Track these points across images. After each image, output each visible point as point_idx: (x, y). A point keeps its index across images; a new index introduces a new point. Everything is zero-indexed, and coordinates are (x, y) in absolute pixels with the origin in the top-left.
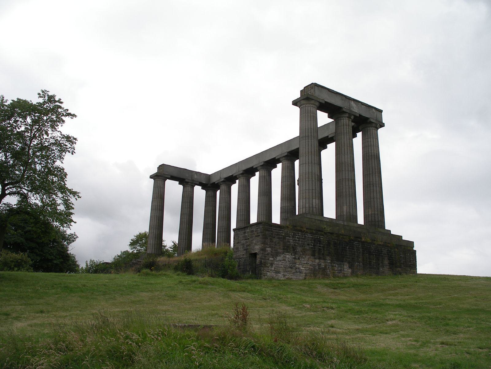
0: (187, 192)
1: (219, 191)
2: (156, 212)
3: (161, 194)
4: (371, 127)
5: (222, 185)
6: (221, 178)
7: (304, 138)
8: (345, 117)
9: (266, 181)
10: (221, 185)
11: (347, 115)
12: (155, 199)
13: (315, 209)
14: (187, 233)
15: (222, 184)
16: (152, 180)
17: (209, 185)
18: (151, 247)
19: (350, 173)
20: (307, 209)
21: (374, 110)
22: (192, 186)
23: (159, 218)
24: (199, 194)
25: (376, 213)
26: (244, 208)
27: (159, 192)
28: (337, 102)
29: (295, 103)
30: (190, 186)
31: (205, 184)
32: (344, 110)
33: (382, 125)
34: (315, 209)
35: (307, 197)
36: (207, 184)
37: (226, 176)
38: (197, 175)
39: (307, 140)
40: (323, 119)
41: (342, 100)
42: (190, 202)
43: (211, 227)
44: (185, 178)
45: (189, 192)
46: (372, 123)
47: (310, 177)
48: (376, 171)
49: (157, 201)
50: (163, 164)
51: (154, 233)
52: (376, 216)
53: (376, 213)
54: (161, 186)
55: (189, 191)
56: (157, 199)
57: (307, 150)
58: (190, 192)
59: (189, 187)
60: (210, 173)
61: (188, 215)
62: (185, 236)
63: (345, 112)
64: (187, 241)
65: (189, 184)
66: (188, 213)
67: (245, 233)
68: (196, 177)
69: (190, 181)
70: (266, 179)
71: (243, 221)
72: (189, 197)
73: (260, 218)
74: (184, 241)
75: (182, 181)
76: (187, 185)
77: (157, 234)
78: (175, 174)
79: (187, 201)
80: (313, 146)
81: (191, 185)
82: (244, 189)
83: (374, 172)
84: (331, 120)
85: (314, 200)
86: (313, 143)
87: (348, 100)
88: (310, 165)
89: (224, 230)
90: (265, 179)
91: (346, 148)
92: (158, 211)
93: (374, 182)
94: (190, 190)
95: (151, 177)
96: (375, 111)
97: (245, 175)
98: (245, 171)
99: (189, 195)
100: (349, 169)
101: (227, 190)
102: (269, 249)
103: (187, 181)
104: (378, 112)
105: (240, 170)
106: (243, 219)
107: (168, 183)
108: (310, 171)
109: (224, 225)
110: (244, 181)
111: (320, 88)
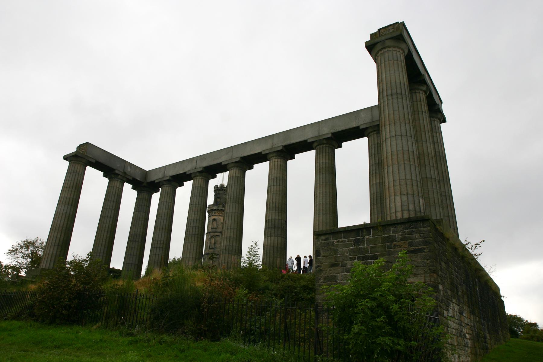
0: (115, 188)
2: (66, 208)
3: (78, 183)
4: (436, 118)
5: (165, 186)
6: (164, 177)
7: (395, 96)
8: (422, 90)
9: (240, 184)
10: (164, 185)
12: (68, 189)
14: (107, 243)
15: (165, 183)
16: (67, 163)
17: (144, 184)
18: (49, 260)
22: (123, 181)
23: (69, 216)
26: (198, 218)
27: (76, 180)
30: (119, 180)
31: (139, 180)
33: (444, 121)
35: (410, 192)
36: (142, 183)
38: (131, 168)
39: (400, 100)
42: (116, 202)
43: (140, 240)
44: (114, 168)
45: (117, 189)
47: (412, 160)
49: (70, 192)
50: (87, 143)
51: (58, 239)
54: (79, 172)
55: (118, 186)
56: (70, 190)
57: (402, 116)
58: (119, 188)
59: (118, 181)
60: (147, 168)
61: (112, 219)
62: (103, 248)
64: (105, 255)
65: (119, 176)
66: (112, 216)
67: (357, 242)
68: (129, 169)
69: (120, 174)
70: (240, 181)
71: (196, 236)
72: (116, 194)
73: (229, 233)
74: (101, 255)
76: (116, 179)
77: (62, 239)
78: (102, 160)
79: (112, 200)
81: (121, 180)
82: (201, 192)
89: (161, 245)
90: (239, 181)
91: (423, 133)
92: (70, 206)
93: (447, 194)
94: (119, 186)
95: (66, 158)
97: (204, 174)
98: (205, 168)
99: (117, 191)
101: (171, 192)
103: (117, 172)
105: (198, 166)
106: (196, 234)
107: (90, 171)
109: (162, 239)
110: (202, 181)
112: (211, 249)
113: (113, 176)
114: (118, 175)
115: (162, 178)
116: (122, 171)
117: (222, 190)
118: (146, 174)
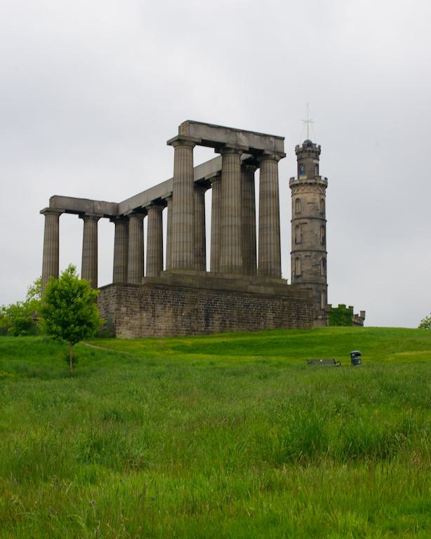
1: (147, 217)
11: (233, 151)
13: (185, 263)
17: (117, 217)
19: (233, 218)
20: (178, 263)
21: (272, 139)
24: (106, 229)
25: (269, 260)
28: (220, 137)
29: (169, 143)
32: (228, 146)
34: (185, 263)
35: (178, 250)
36: (115, 216)
37: (135, 206)
38: (100, 205)
39: (182, 187)
40: (203, 155)
41: (226, 134)
46: (267, 155)
48: (272, 211)
52: (269, 264)
53: (269, 260)
63: (230, 149)
68: (99, 208)
69: (91, 214)
75: (82, 215)
78: (70, 208)
80: (185, 193)
83: (269, 213)
84: (219, 155)
85: (185, 254)
86: (185, 191)
87: (234, 133)
88: (182, 215)
93: (268, 226)
95: (42, 212)
96: (273, 140)
100: (233, 214)
102: (124, 309)
103: (87, 214)
104: (278, 142)
108: (182, 222)
111: (196, 125)
112: (298, 244)
113: (85, 218)
114: (89, 216)
115: (127, 212)
116: (92, 211)
117: (306, 151)
118: (116, 207)
